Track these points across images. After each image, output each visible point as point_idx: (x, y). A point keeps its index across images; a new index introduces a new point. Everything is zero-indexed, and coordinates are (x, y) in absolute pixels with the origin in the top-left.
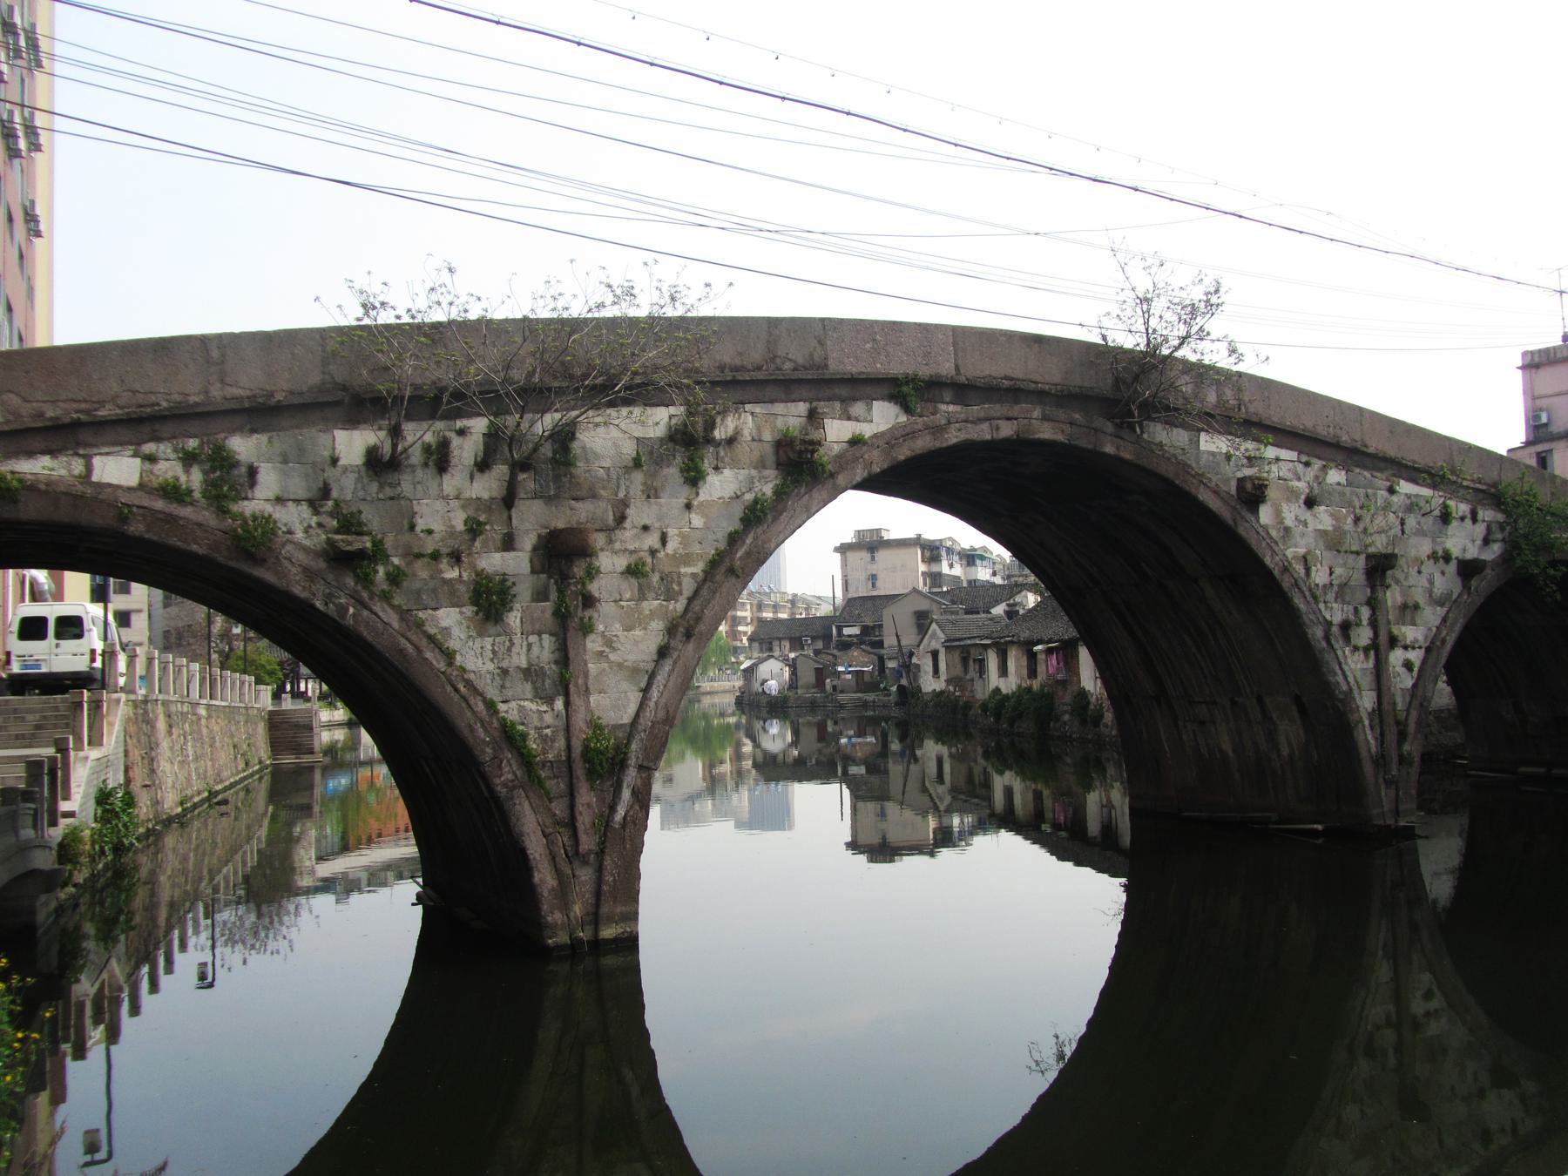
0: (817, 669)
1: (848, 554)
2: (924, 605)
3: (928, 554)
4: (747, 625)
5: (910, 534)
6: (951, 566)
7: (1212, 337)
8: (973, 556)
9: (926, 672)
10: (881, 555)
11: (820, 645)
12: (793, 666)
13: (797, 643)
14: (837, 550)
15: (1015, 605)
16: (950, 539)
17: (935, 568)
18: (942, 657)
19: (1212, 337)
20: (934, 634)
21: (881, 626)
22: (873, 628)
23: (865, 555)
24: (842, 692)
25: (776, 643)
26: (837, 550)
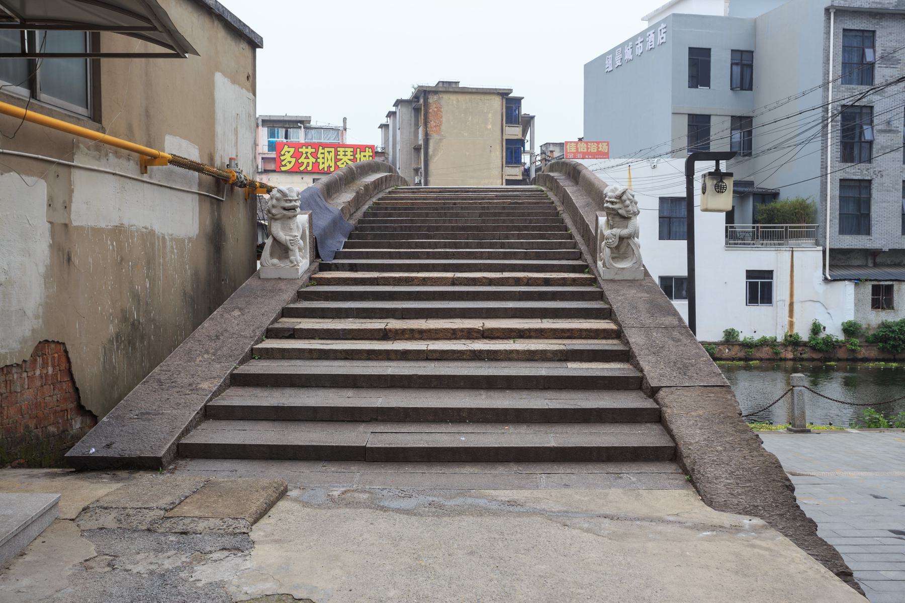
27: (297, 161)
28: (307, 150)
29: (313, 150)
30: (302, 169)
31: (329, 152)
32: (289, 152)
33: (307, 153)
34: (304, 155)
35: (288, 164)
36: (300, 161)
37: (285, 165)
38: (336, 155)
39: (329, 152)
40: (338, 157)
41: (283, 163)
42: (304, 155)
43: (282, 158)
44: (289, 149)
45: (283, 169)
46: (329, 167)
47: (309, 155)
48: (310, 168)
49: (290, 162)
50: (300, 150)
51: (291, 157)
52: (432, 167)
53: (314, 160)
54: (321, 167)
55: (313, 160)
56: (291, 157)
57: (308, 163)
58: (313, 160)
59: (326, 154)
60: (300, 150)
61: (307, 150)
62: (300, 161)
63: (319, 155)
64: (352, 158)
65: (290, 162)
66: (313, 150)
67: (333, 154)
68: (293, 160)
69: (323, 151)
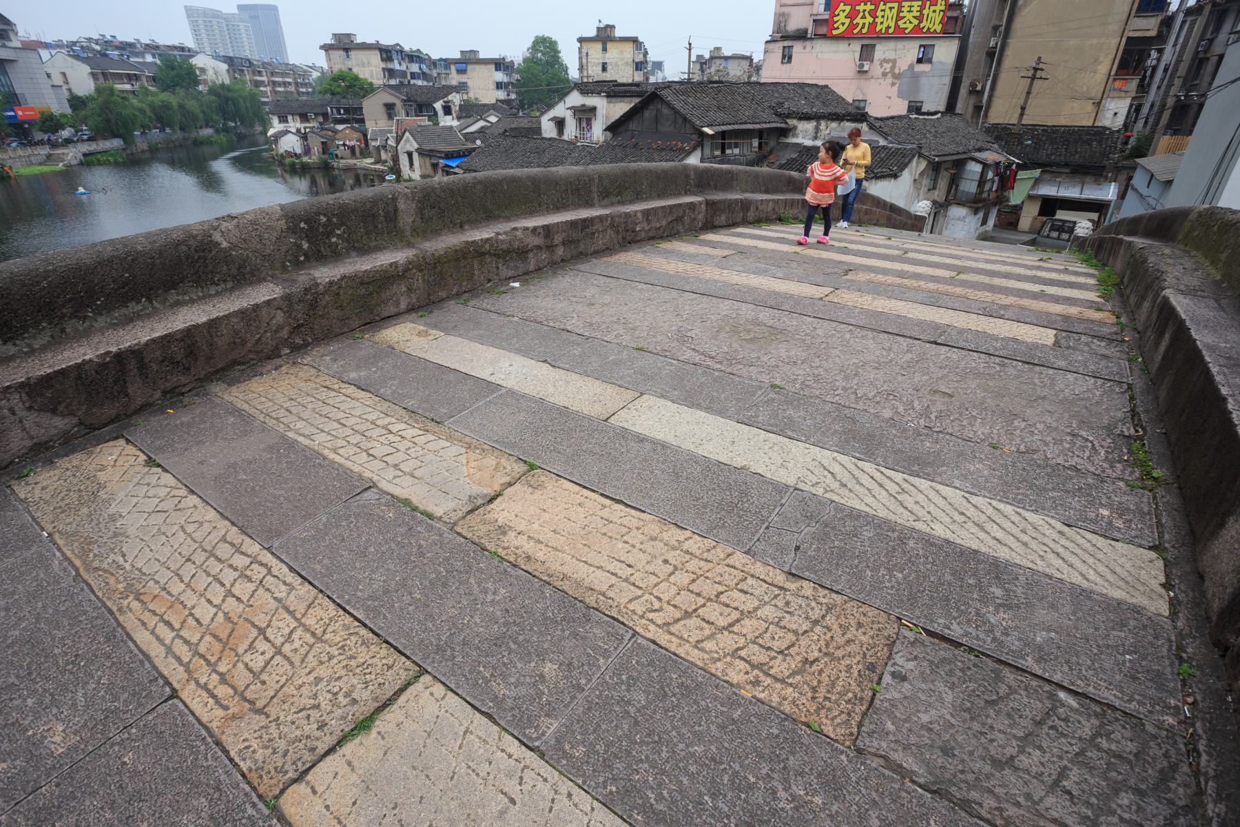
0: (323, 143)
1: (330, 52)
2: (391, 99)
3: (384, 56)
4: (266, 86)
5: (370, 40)
6: (400, 64)
7: (1091, 101)
8: (412, 56)
9: (405, 166)
10: (353, 54)
11: (321, 119)
12: (304, 137)
13: (304, 118)
14: (322, 47)
15: (448, 102)
16: (398, 44)
17: (390, 66)
18: (415, 156)
19: (1091, 101)
20: (408, 138)
21: (361, 108)
22: (356, 109)
23: (342, 53)
24: (342, 158)
25: (290, 118)
26: (322, 47)
27: (851, 22)
28: (865, 7)
29: (873, 7)
30: (855, 32)
31: (891, 8)
32: (844, 11)
33: (864, 11)
34: (861, 14)
35: (841, 26)
36: (855, 22)
37: (838, 28)
38: (899, 11)
39: (891, 8)
40: (901, 14)
41: (836, 26)
42: (861, 14)
43: (835, 19)
44: (844, 8)
45: (835, 32)
46: (888, 27)
47: (866, 13)
48: (864, 31)
49: (843, 24)
50: (857, 8)
51: (846, 17)
52: (1018, 24)
53: (871, 20)
54: (878, 29)
55: (869, 19)
56: (846, 17)
57: (864, 24)
58: (869, 19)
59: (888, 11)
60: (857, 8)
61: (865, 7)
62: (855, 22)
63: (879, 13)
64: (918, 14)
65: (843, 24)
66: (873, 7)
67: (895, 11)
68: (848, 21)
69: (883, 8)
